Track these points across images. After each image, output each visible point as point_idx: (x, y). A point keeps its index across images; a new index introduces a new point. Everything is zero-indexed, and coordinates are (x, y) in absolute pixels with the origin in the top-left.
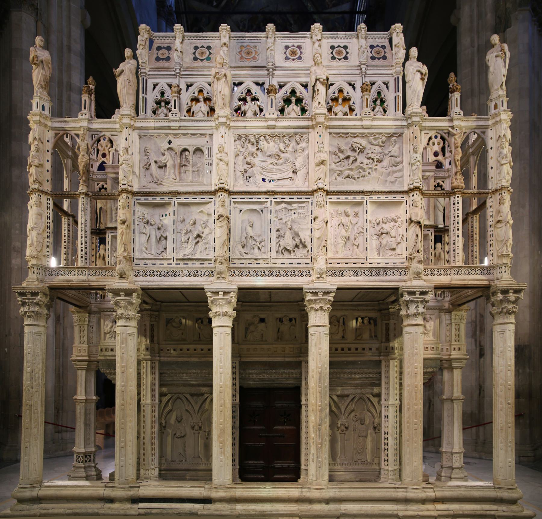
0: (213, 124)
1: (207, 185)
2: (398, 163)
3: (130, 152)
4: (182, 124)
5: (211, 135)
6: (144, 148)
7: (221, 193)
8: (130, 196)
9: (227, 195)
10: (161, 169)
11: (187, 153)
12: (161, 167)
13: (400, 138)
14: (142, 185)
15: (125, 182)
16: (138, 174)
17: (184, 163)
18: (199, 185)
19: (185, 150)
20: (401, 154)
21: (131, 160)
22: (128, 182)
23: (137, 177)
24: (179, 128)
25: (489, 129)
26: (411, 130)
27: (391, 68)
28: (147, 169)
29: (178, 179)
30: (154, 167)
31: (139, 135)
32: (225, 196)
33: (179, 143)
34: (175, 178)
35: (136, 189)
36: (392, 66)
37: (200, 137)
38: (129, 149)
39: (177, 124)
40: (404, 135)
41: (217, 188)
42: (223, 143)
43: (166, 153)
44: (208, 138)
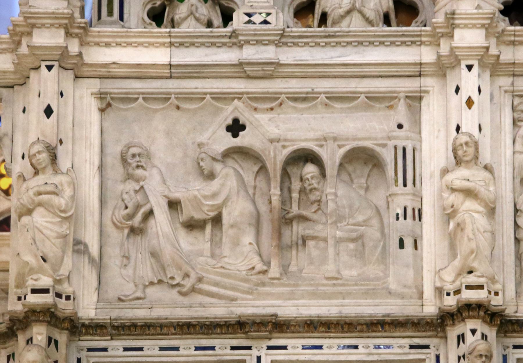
0: (427, 55)
1: (402, 296)
3: (64, 163)
4: (289, 56)
5: (415, 99)
6: (119, 149)
7: (470, 324)
8: (62, 337)
9: (492, 333)
10: (196, 233)
11: (310, 169)
12: (193, 226)
14: (112, 294)
15: (45, 281)
16: (94, 250)
17: (295, 210)
18: (368, 294)
19: (306, 157)
21: (68, 192)
22: (58, 282)
23: (91, 260)
24: (271, 70)
28: (133, 231)
29: (275, 271)
30: (162, 218)
31: (101, 96)
32: (484, 337)
33: (276, 131)
34: (260, 266)
35: (88, 309)
37: (367, 108)
38: (61, 151)
39: (269, 53)
41: (451, 302)
42: (469, 126)
43: (218, 167)
44: (401, 113)
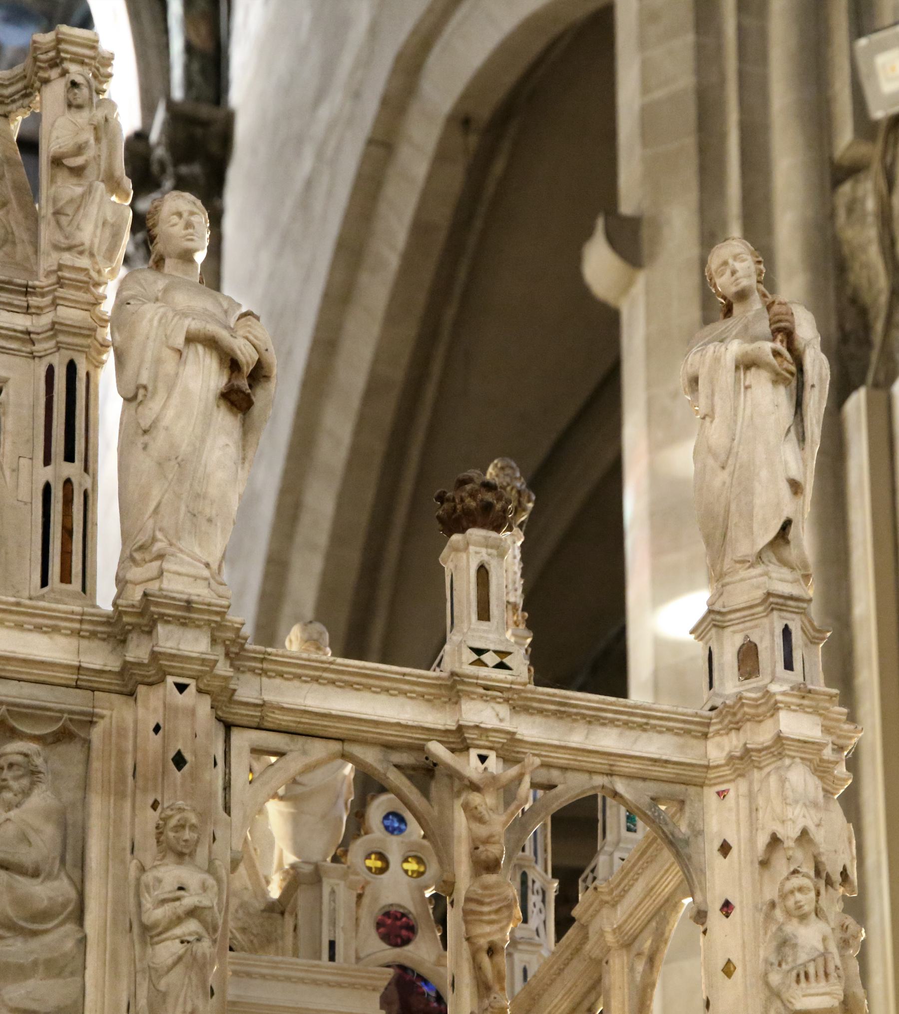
2: (44, 915)
13: (61, 748)
20: (73, 858)
25: (710, 794)
26: (152, 704)
27: (20, 300)
36: (27, 291)
40: (96, 734)
